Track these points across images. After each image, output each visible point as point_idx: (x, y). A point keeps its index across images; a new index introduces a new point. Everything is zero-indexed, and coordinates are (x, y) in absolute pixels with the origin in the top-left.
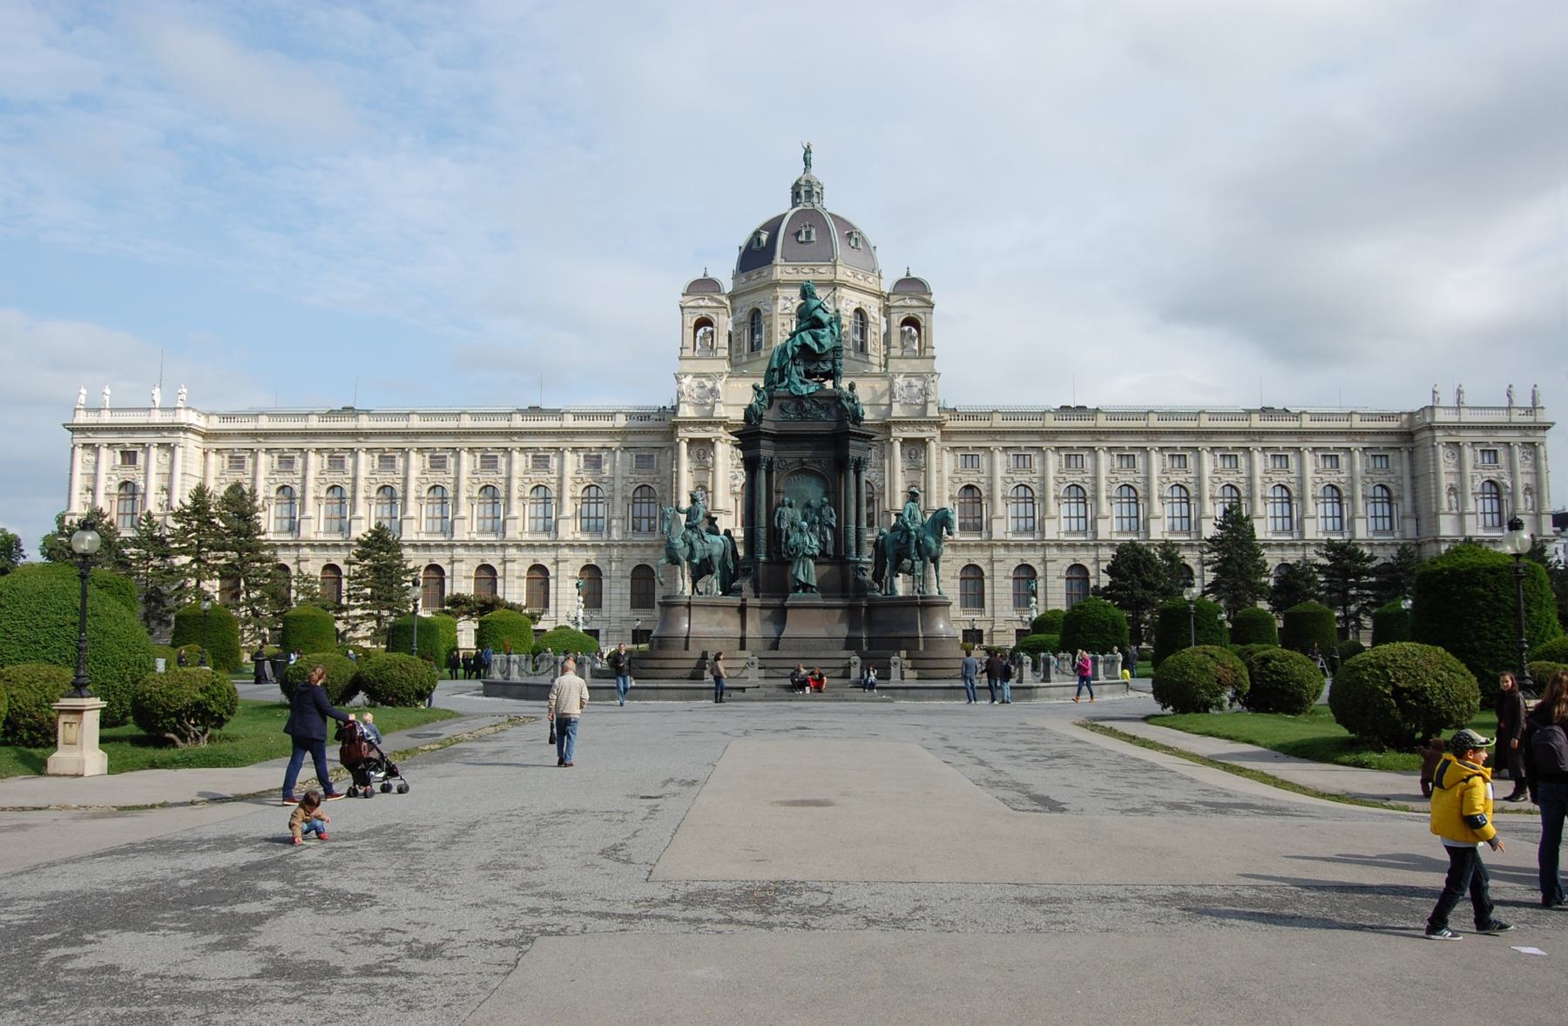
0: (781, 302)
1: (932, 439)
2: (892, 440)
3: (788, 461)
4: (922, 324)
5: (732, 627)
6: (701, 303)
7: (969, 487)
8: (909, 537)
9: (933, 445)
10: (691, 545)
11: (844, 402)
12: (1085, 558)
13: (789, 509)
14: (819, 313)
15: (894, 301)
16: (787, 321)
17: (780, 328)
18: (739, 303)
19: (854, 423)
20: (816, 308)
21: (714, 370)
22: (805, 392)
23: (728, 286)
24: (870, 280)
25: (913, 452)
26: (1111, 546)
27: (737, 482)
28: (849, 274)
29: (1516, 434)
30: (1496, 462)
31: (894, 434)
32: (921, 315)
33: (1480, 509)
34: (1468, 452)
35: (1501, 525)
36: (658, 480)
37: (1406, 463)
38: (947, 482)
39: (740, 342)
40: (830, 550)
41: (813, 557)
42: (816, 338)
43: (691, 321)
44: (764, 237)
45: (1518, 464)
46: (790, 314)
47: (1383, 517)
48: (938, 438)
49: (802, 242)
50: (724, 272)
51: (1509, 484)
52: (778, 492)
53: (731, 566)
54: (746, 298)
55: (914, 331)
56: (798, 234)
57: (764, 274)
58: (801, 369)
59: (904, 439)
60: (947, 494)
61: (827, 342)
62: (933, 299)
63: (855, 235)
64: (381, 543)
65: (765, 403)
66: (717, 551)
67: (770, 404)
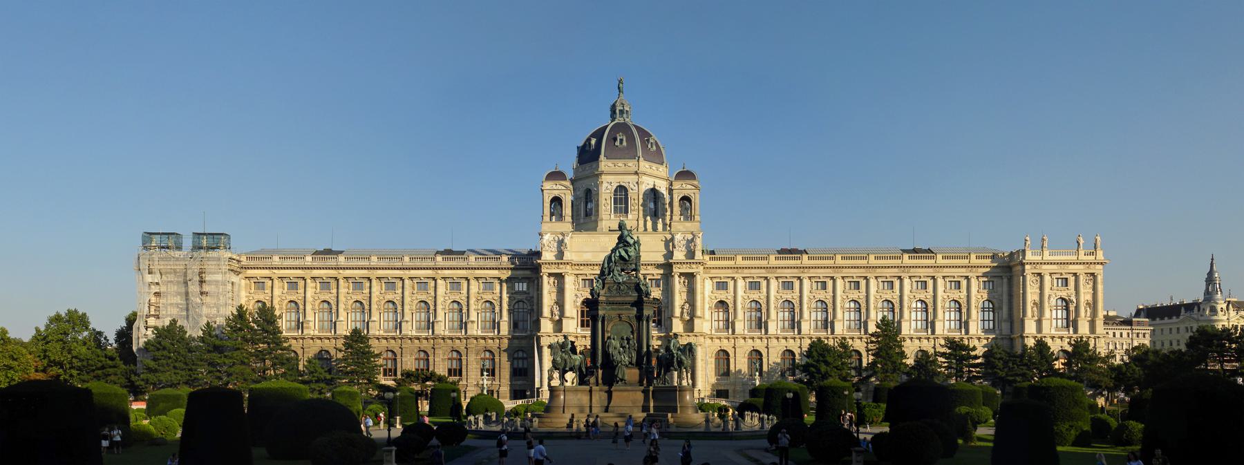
0: (605, 185)
4: (693, 200)
5: (585, 399)
6: (555, 187)
7: (722, 302)
8: (674, 357)
10: (565, 360)
11: (641, 286)
12: (794, 346)
13: (613, 341)
14: (628, 239)
15: (677, 185)
17: (604, 202)
18: (578, 184)
19: (646, 297)
22: (621, 281)
23: (570, 174)
26: (811, 338)
27: (578, 299)
28: (648, 167)
29: (1081, 267)
30: (1067, 286)
31: (674, 270)
33: (1054, 316)
34: (1047, 279)
35: (1068, 326)
36: (529, 298)
37: (1005, 288)
38: (707, 299)
39: (578, 210)
40: (634, 360)
42: (626, 252)
45: (1081, 286)
47: (989, 320)
48: (702, 272)
50: (569, 165)
51: (1074, 300)
52: (608, 332)
53: (584, 370)
55: (688, 204)
56: (615, 139)
60: (707, 306)
61: (632, 254)
63: (651, 141)
64: (357, 339)
65: (601, 287)
66: (577, 363)
67: (603, 288)
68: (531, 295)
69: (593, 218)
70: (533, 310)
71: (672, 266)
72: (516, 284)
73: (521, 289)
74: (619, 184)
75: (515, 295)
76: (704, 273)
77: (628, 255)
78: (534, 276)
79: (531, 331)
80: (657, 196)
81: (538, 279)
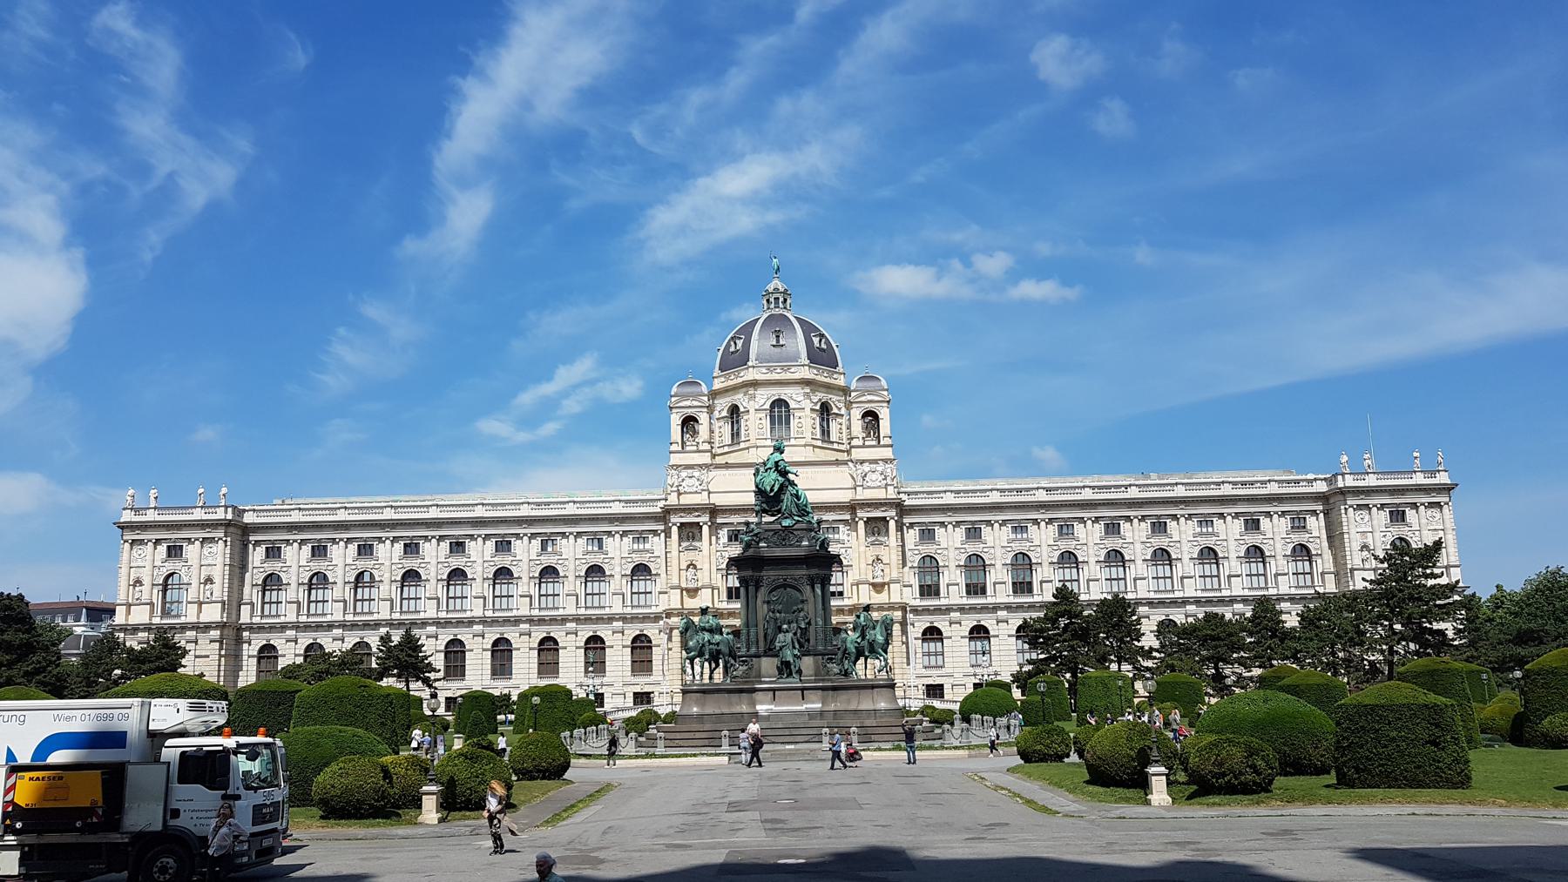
2: (857, 519)
9: (892, 524)
16: (762, 415)
31: (859, 515)
44: (740, 343)
46: (765, 410)
49: (774, 346)
57: (742, 374)
69: (742, 445)
71: (855, 509)
75: (633, 555)
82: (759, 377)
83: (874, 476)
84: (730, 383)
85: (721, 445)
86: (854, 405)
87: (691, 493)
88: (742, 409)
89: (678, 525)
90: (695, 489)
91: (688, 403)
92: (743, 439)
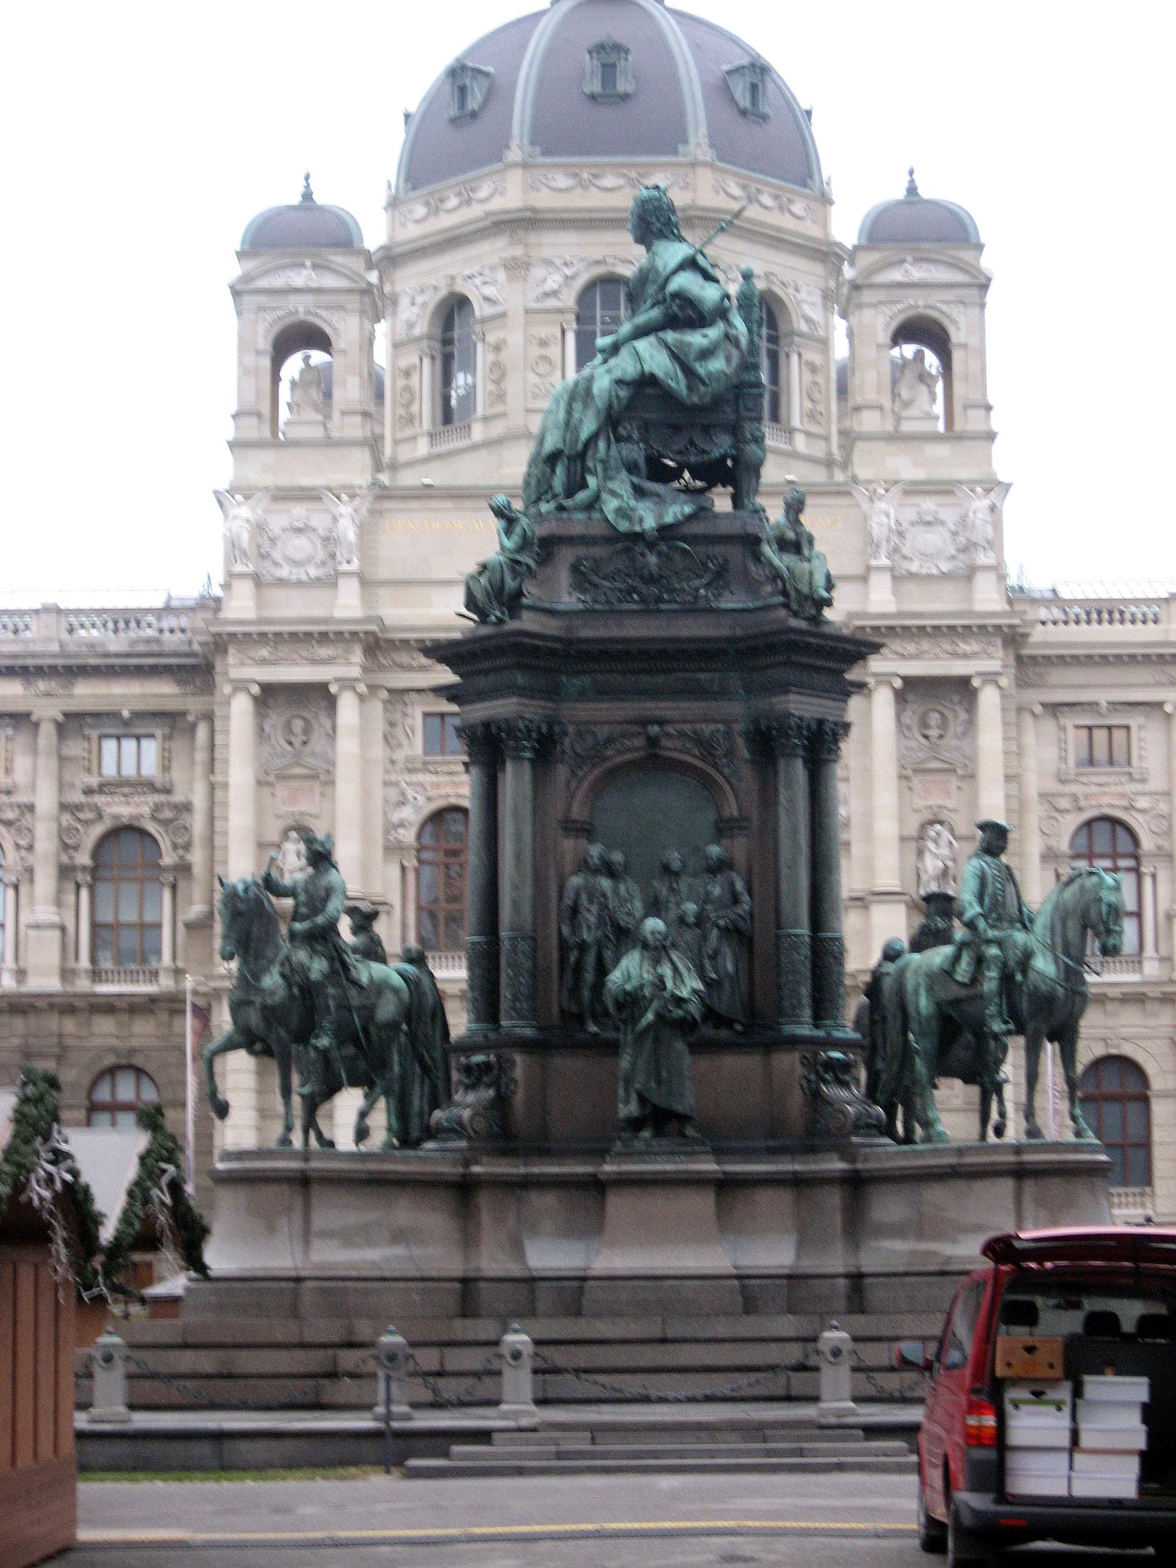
1: (990, 678)
3: (603, 731)
4: (957, 336)
6: (300, 278)
9: (989, 700)
20: (681, 267)
21: (335, 478)
24: (798, 208)
25: (934, 718)
32: (956, 312)
36: (167, 814)
41: (685, 1026)
43: (264, 343)
46: (560, 311)
49: (593, 97)
54: (424, 265)
55: (931, 360)
57: (483, 193)
58: (635, 452)
59: (907, 680)
62: (986, 262)
66: (387, 1009)
68: (178, 797)
69: (478, 432)
70: (185, 868)
72: (110, 746)
73: (129, 770)
74: (600, 270)
75: (100, 800)
76: (1022, 683)
77: (688, 372)
78: (193, 705)
79: (178, 973)
80: (783, 327)
81: (209, 717)
82: (544, 200)
83: (933, 539)
84: (446, 221)
85: (408, 432)
86: (868, 296)
87: (299, 584)
88: (480, 309)
89: (256, 690)
90: (313, 572)
91: (300, 278)
92: (480, 410)
